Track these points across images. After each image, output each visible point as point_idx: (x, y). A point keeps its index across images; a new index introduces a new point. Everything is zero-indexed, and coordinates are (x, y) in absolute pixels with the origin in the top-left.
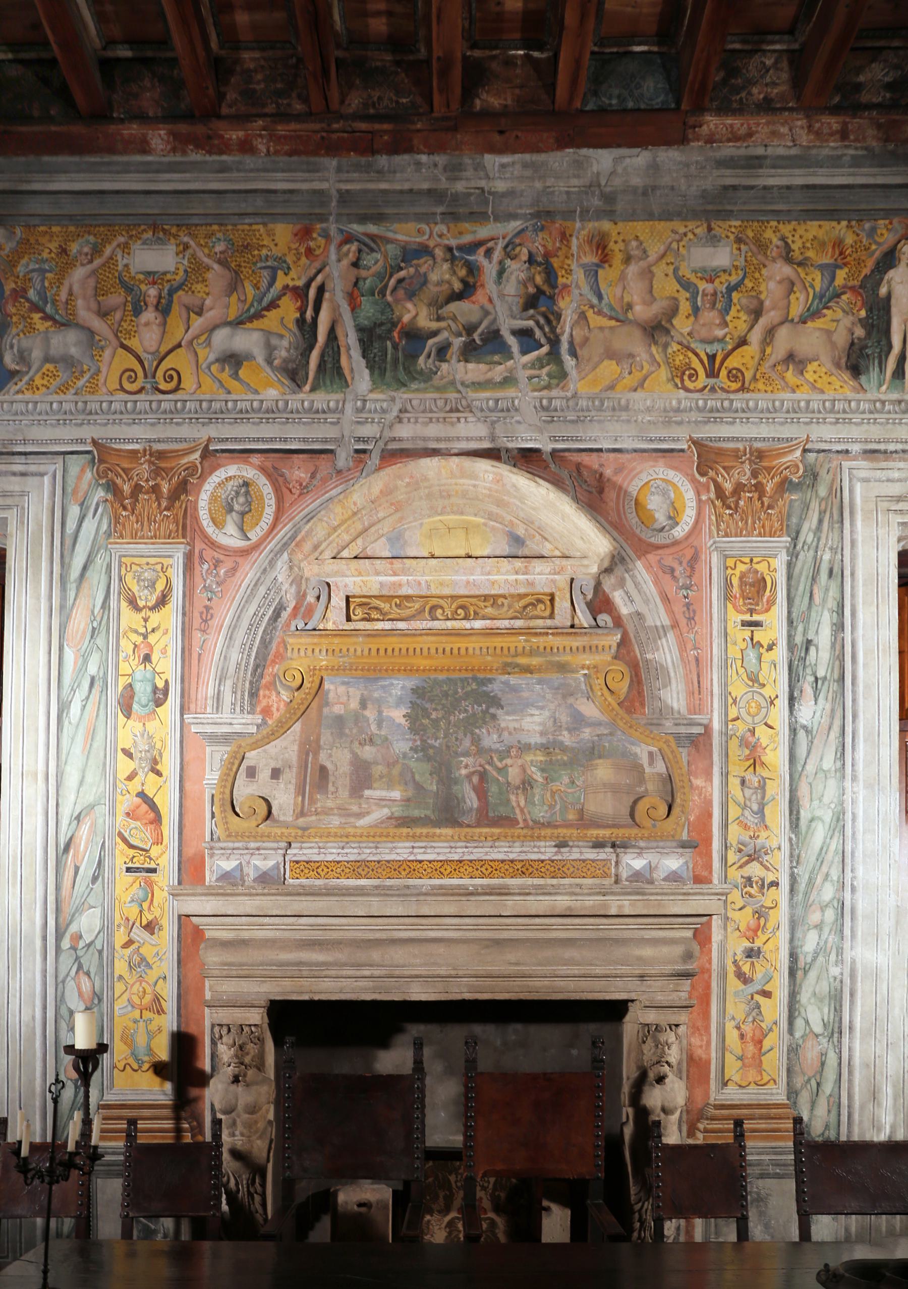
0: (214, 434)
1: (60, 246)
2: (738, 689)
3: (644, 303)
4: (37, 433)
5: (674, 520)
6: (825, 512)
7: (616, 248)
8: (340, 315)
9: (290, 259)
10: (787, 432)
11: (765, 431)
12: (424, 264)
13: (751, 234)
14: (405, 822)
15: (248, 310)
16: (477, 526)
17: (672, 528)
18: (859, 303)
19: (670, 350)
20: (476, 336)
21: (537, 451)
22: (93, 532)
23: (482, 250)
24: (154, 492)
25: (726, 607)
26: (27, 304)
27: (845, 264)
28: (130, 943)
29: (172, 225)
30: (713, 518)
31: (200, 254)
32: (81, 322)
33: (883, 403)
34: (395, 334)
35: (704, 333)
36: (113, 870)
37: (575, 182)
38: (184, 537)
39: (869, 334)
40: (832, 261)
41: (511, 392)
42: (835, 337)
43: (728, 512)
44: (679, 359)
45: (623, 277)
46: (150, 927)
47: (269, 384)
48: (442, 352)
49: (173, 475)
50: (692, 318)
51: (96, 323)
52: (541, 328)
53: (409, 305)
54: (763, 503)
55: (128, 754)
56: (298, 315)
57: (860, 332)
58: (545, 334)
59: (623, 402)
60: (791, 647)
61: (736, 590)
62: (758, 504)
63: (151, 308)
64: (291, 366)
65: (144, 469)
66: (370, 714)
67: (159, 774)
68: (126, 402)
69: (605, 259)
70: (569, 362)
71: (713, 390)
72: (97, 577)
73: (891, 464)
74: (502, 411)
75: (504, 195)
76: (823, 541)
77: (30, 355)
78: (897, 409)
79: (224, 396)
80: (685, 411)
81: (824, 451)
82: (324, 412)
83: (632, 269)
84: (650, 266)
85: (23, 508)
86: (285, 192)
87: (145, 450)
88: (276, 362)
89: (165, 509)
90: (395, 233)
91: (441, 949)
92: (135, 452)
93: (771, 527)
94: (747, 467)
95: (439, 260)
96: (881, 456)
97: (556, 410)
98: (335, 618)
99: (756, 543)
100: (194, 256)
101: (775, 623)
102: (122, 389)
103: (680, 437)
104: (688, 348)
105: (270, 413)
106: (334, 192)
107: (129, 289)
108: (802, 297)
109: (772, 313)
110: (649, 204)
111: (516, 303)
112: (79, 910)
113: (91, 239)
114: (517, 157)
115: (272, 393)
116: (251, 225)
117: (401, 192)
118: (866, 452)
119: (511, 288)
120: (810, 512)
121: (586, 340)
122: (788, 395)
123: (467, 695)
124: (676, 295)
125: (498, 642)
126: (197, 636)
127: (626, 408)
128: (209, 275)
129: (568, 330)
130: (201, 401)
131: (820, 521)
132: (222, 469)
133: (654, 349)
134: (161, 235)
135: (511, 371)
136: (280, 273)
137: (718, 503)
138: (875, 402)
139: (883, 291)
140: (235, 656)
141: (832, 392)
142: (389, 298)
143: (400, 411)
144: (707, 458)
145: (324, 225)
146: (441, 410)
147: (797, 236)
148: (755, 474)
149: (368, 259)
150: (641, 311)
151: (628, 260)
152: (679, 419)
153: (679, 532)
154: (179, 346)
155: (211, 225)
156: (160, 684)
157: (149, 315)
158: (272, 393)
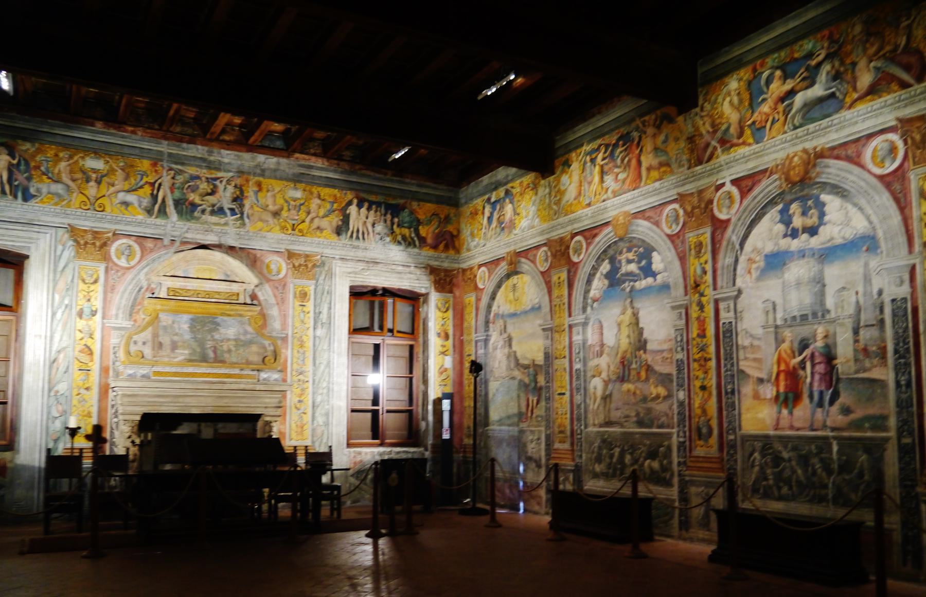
2: (298, 324)
4: (49, 219)
5: (279, 272)
9: (148, 172)
10: (316, 250)
12: (198, 182)
28: (78, 394)
35: (291, 217)
41: (226, 228)
44: (283, 224)
45: (266, 196)
46: (87, 389)
47: (139, 214)
48: (203, 211)
55: (80, 331)
57: (340, 223)
60: (315, 313)
65: (89, 237)
66: (176, 326)
69: (260, 190)
70: (246, 220)
72: (69, 271)
83: (269, 194)
99: (305, 282)
105: (140, 224)
110: (276, 174)
111: (230, 199)
112: (59, 382)
115: (140, 217)
123: (209, 322)
126: (109, 295)
140: (124, 302)
144: (291, 255)
149: (178, 177)
150: (271, 208)
151: (268, 191)
153: (281, 276)
157: (92, 183)
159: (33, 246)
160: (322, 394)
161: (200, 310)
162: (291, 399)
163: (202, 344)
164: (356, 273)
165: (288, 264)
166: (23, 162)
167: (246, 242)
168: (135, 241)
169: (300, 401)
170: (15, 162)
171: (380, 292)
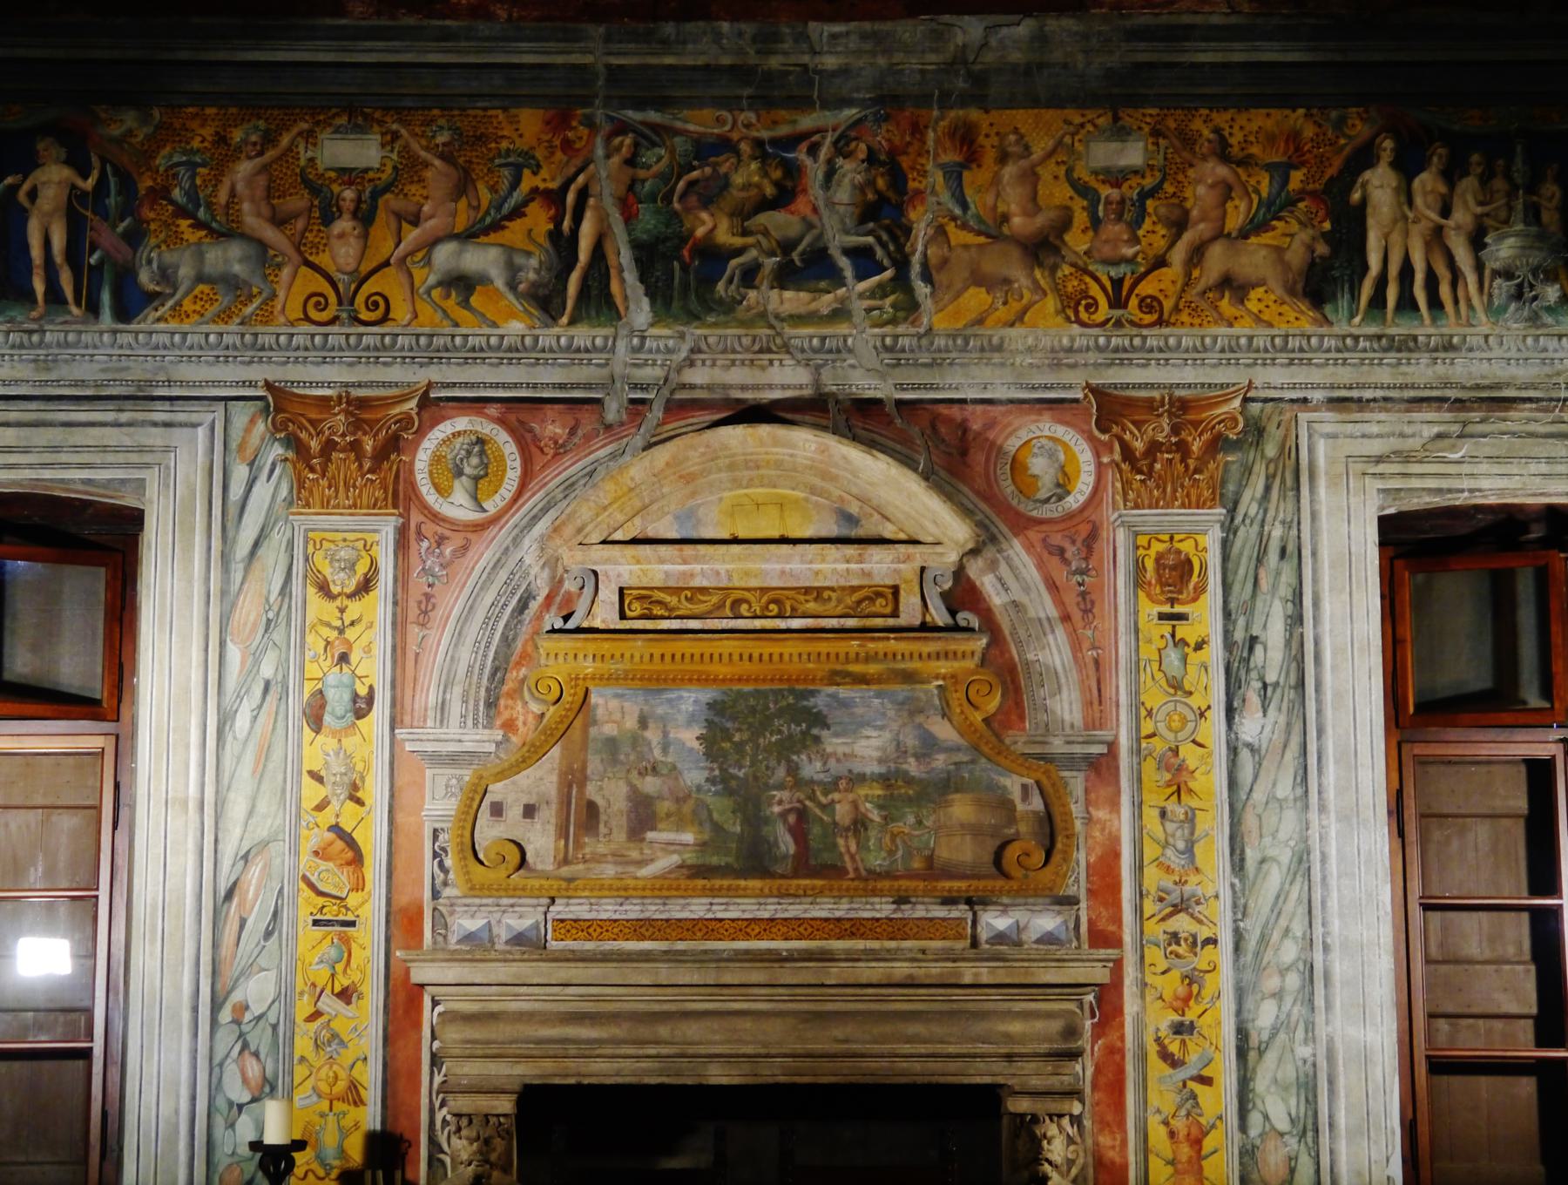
0: (436, 378)
1: (217, 133)
2: (1155, 697)
3: (1026, 213)
5: (1063, 488)
6: (1274, 476)
7: (987, 143)
8: (609, 226)
9: (539, 154)
11: (1189, 375)
13: (1173, 125)
14: (699, 871)
15: (483, 219)
16: (797, 501)
17: (1060, 499)
18: (1321, 213)
19: (1060, 274)
20: (795, 256)
21: (877, 402)
22: (268, 499)
23: (804, 146)
24: (352, 450)
25: (1136, 596)
26: (170, 208)
27: (1303, 164)
28: (316, 1015)
29: (376, 108)
30: (1119, 485)
31: (415, 146)
32: (248, 231)
33: (1356, 338)
34: (686, 253)
35: (1107, 251)
36: (295, 924)
37: (932, 58)
38: (395, 506)
39: (1335, 252)
40: (1284, 159)
41: (842, 329)
42: (1288, 256)
43: (1138, 477)
45: (996, 180)
46: (345, 995)
47: (513, 315)
48: (749, 276)
49: (380, 430)
50: (1091, 233)
51: (270, 234)
52: (883, 245)
53: (704, 216)
54: (1187, 467)
55: (317, 777)
56: (551, 226)
57: (1322, 249)
58: (889, 254)
59: (995, 340)
60: (1229, 644)
61: (1150, 574)
62: (1181, 468)
63: (346, 216)
64: (541, 292)
65: (339, 420)
66: (653, 735)
67: (360, 802)
68: (313, 336)
69: (972, 158)
70: (922, 289)
71: (1119, 324)
72: (273, 556)
73: (1367, 416)
74: (830, 351)
75: (833, 74)
76: (1271, 513)
77: (176, 272)
78: (1376, 346)
79: (449, 330)
80: (1080, 350)
81: (1272, 400)
82: (587, 351)
83: (1009, 171)
84: (1033, 166)
85: (168, 468)
86: (533, 66)
87: (340, 397)
88: (522, 287)
89: (369, 471)
90: (686, 122)
91: (748, 1024)
92: (325, 400)
93: (1199, 497)
94: (1165, 422)
95: (745, 157)
96: (1354, 406)
97: (903, 350)
98: (604, 615)
99: (1177, 517)
100: (406, 147)
101: (1205, 616)
102: (307, 319)
103: (1073, 383)
104: (1086, 271)
105: (514, 353)
106: (600, 68)
107: (315, 190)
108: (1243, 206)
109: (1202, 226)
110: (1033, 86)
112: (246, 973)
113: (262, 124)
114: (853, 25)
115: (516, 327)
116: (485, 109)
117: (694, 68)
118: (1331, 400)
119: (843, 194)
120: (1253, 477)
121: (945, 262)
122: (1223, 330)
123: (780, 713)
124: (1069, 203)
125: (823, 647)
126: (414, 631)
127: (999, 348)
128: (428, 174)
129: (920, 248)
130: (418, 336)
131: (1268, 489)
132: (448, 422)
133: (1038, 274)
134: (360, 120)
135: (842, 301)
136: (526, 172)
137: (1125, 467)
138: (1344, 337)
139: (1356, 196)
140: (465, 655)
141: (1284, 326)
142: (676, 206)
143: (692, 351)
144: (1109, 410)
145: (587, 111)
146: (747, 350)
147: (1236, 128)
148: (1175, 430)
149: (648, 157)
151: (1003, 158)
152: (1071, 361)
153: (1074, 501)
154: (387, 264)
155: (430, 109)
156: (363, 691)
157: (344, 224)
158: (516, 327)
159: (152, 477)
160: (1278, 995)
161: (746, 668)
162: (1144, 1015)
163: (749, 802)
164: (1406, 457)
165: (1098, 449)
166: (112, 180)
167: (924, 377)
168: (501, 421)
169: (1179, 1029)
170: (88, 185)
171: (1536, 532)
